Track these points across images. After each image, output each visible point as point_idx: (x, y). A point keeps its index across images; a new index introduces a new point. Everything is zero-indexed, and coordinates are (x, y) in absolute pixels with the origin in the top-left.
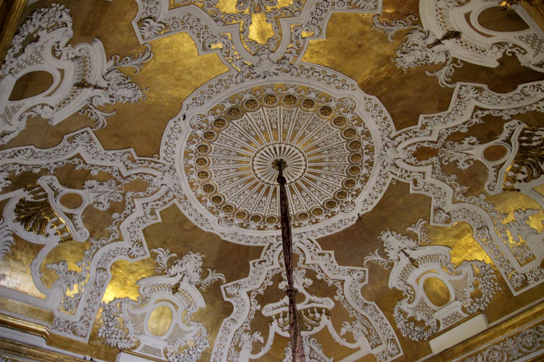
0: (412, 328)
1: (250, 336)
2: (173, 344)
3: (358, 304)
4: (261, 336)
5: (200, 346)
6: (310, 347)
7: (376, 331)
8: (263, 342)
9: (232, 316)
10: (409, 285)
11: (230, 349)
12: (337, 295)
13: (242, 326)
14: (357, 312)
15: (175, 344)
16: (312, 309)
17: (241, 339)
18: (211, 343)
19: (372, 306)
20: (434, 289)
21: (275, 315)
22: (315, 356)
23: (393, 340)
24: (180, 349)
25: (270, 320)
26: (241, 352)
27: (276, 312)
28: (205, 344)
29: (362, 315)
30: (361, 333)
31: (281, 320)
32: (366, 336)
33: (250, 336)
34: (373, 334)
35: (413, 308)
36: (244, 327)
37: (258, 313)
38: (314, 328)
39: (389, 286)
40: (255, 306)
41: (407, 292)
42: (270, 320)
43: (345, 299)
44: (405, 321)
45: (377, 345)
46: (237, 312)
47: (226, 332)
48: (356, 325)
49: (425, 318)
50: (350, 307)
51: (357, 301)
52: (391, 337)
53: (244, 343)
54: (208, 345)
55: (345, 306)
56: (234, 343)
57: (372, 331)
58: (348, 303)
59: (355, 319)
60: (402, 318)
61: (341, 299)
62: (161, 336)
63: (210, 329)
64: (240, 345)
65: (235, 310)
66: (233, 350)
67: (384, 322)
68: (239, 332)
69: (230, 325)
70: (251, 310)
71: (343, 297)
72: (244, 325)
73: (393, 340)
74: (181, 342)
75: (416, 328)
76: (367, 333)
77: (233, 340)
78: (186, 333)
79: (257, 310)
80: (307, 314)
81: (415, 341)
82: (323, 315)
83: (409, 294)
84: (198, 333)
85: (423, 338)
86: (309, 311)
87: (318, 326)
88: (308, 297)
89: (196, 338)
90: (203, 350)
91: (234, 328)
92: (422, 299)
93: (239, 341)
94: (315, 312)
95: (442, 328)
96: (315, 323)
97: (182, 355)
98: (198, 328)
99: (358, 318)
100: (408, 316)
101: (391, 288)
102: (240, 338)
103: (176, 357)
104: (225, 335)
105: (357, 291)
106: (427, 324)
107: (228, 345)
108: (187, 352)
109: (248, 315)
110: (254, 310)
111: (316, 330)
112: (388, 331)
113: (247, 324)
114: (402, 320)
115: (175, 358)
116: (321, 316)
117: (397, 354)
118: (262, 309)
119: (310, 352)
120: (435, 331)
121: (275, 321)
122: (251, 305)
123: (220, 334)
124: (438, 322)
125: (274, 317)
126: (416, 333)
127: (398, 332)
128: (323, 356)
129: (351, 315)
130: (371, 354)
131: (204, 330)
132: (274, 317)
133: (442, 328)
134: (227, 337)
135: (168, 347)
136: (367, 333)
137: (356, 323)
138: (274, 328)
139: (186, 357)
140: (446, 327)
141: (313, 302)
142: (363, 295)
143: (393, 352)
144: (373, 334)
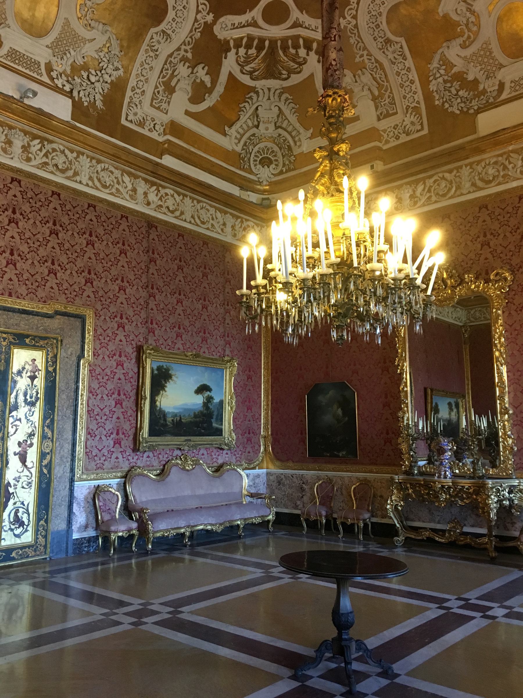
0: (454, 92)
1: (190, 70)
2: (62, 58)
3: (375, 39)
4: (207, 74)
5: (109, 71)
6: (280, 109)
7: (391, 92)
8: (209, 85)
9: (163, 26)
10: (473, 12)
11: (156, 87)
12: (345, 18)
13: (179, 49)
14: (369, 55)
15: (65, 57)
16: (296, 38)
17: (175, 74)
18: (127, 71)
19: (399, 45)
20: (514, 26)
21: (235, 40)
22: (284, 126)
23: (416, 110)
24: (73, 67)
25: (224, 47)
26: (174, 94)
27: (237, 34)
28: (117, 69)
29: (377, 61)
30: (366, 92)
31: (242, 51)
32: (374, 99)
33: (190, 70)
34: (386, 96)
35: (466, 57)
36: (182, 53)
37: (208, 28)
38: (292, 75)
39: (440, 10)
40: (205, 13)
41: (467, 25)
42: (224, 47)
43: (356, 26)
44: (446, 78)
45: (388, 115)
46: (174, 20)
47: (152, 54)
48: (362, 77)
49: (481, 76)
50: (360, 44)
51: (376, 33)
52: (414, 104)
53: (179, 80)
54: (121, 72)
55: (352, 41)
56: (164, 77)
57: (386, 91)
58: (359, 36)
59: (362, 67)
60: (442, 72)
61: (350, 26)
62: (40, 36)
63: (125, 44)
64: (173, 84)
65: (171, 14)
66: (161, 89)
67: (410, 77)
68: (172, 59)
69: (159, 43)
70: (196, 20)
71: (354, 22)
72: (183, 47)
73: (416, 110)
74: (75, 56)
75: (461, 93)
76: (376, 93)
77: (162, 72)
78: (85, 41)
79: (206, 23)
80: (285, 48)
81: (453, 112)
82: (312, 54)
83: (469, 30)
84: (104, 45)
85: (468, 109)
86: (290, 42)
87: (299, 72)
88: (295, 14)
89: (102, 54)
90: (113, 78)
91: (166, 49)
92: (487, 43)
93: (173, 76)
94: (299, 47)
95: (504, 96)
96: (296, 66)
97: (78, 80)
98: (105, 38)
99: (368, 65)
100: (455, 70)
101: (441, 15)
102: (174, 71)
103: (68, 81)
104: (149, 60)
105: (380, 14)
106: (481, 87)
107: (154, 77)
108: (85, 77)
109: (191, 31)
110: (202, 21)
111: (295, 79)
112: (411, 94)
113: (188, 48)
114: (441, 75)
115: (65, 83)
116: (308, 55)
117: (418, 131)
118: (214, 22)
119: (278, 116)
120: (491, 100)
121: (233, 51)
122: (198, 12)
123: (141, 57)
124: (502, 86)
125: (232, 44)
126: (459, 100)
127: (428, 97)
128: (297, 125)
129: (358, 59)
130: (374, 128)
131: (115, 43)
132: (232, 44)
133: (504, 96)
134: (153, 64)
135: (54, 60)
136: (376, 93)
137: (363, 74)
138: (230, 64)
139: (85, 84)
140: (514, 94)
141: (301, 26)
142: (388, 23)
143: (413, 128)
144: (386, 96)
